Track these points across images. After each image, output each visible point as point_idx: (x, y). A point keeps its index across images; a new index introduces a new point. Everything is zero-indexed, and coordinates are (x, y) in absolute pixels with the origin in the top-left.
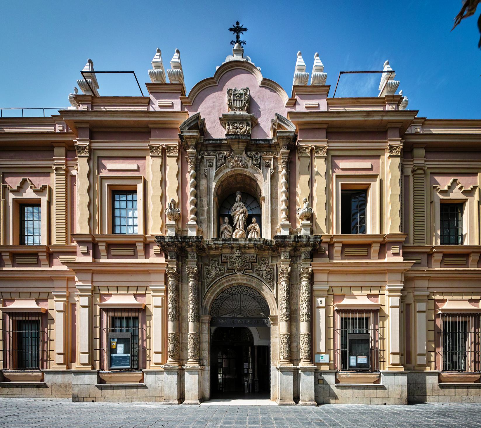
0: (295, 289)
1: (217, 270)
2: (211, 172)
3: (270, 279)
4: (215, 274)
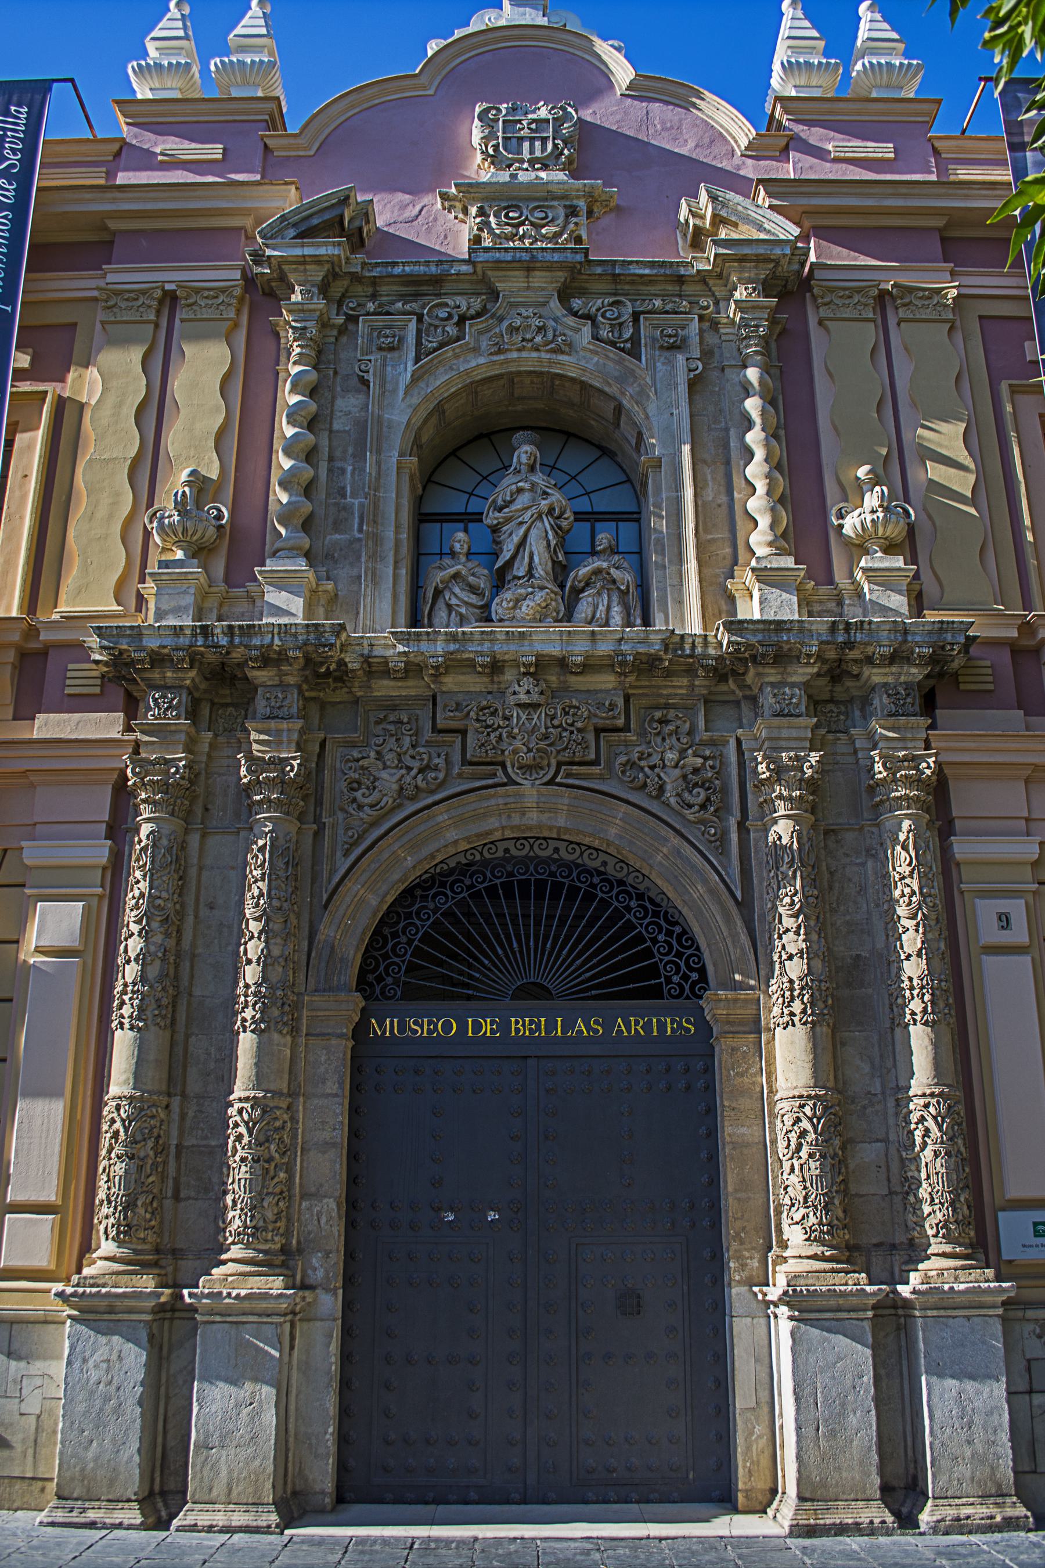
0: (847, 855)
1: (409, 769)
2: (389, 369)
3: (703, 807)
4: (395, 787)
